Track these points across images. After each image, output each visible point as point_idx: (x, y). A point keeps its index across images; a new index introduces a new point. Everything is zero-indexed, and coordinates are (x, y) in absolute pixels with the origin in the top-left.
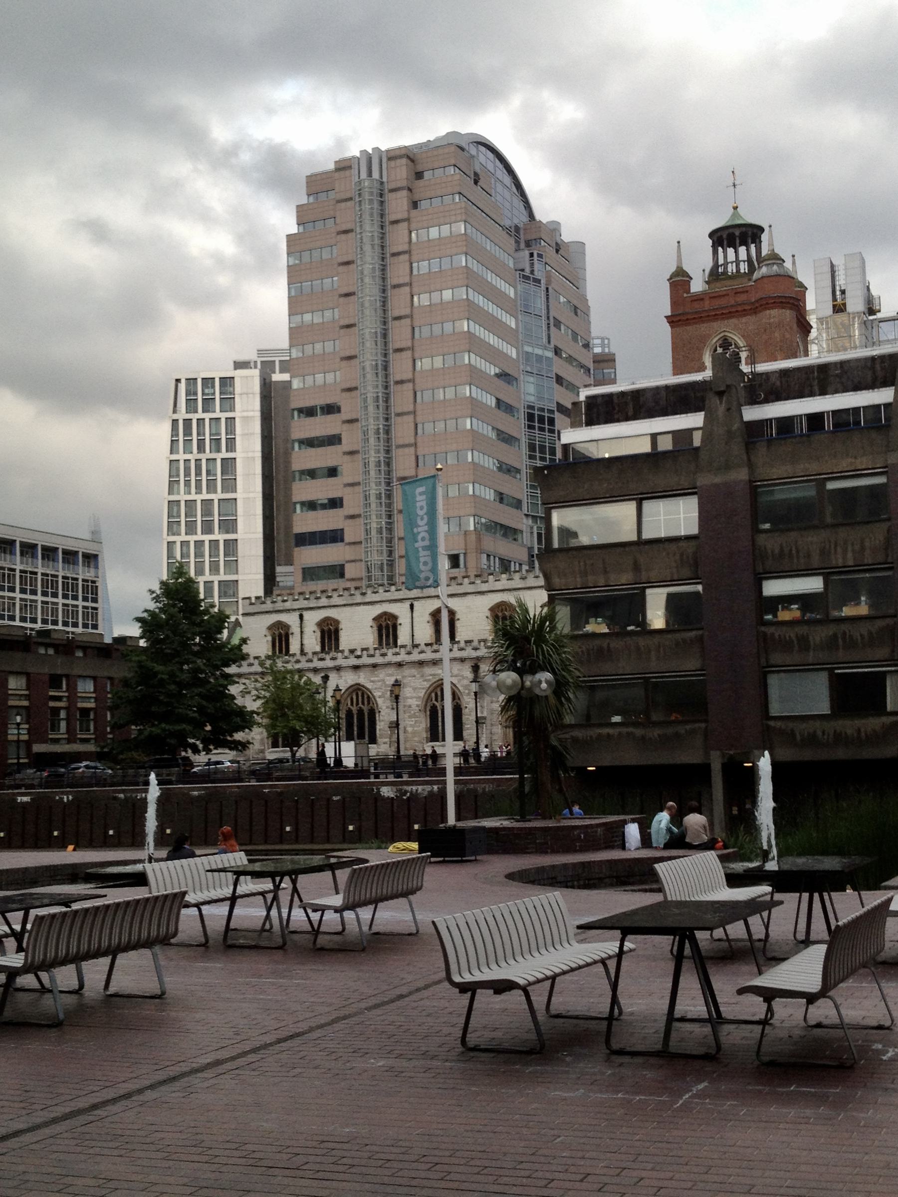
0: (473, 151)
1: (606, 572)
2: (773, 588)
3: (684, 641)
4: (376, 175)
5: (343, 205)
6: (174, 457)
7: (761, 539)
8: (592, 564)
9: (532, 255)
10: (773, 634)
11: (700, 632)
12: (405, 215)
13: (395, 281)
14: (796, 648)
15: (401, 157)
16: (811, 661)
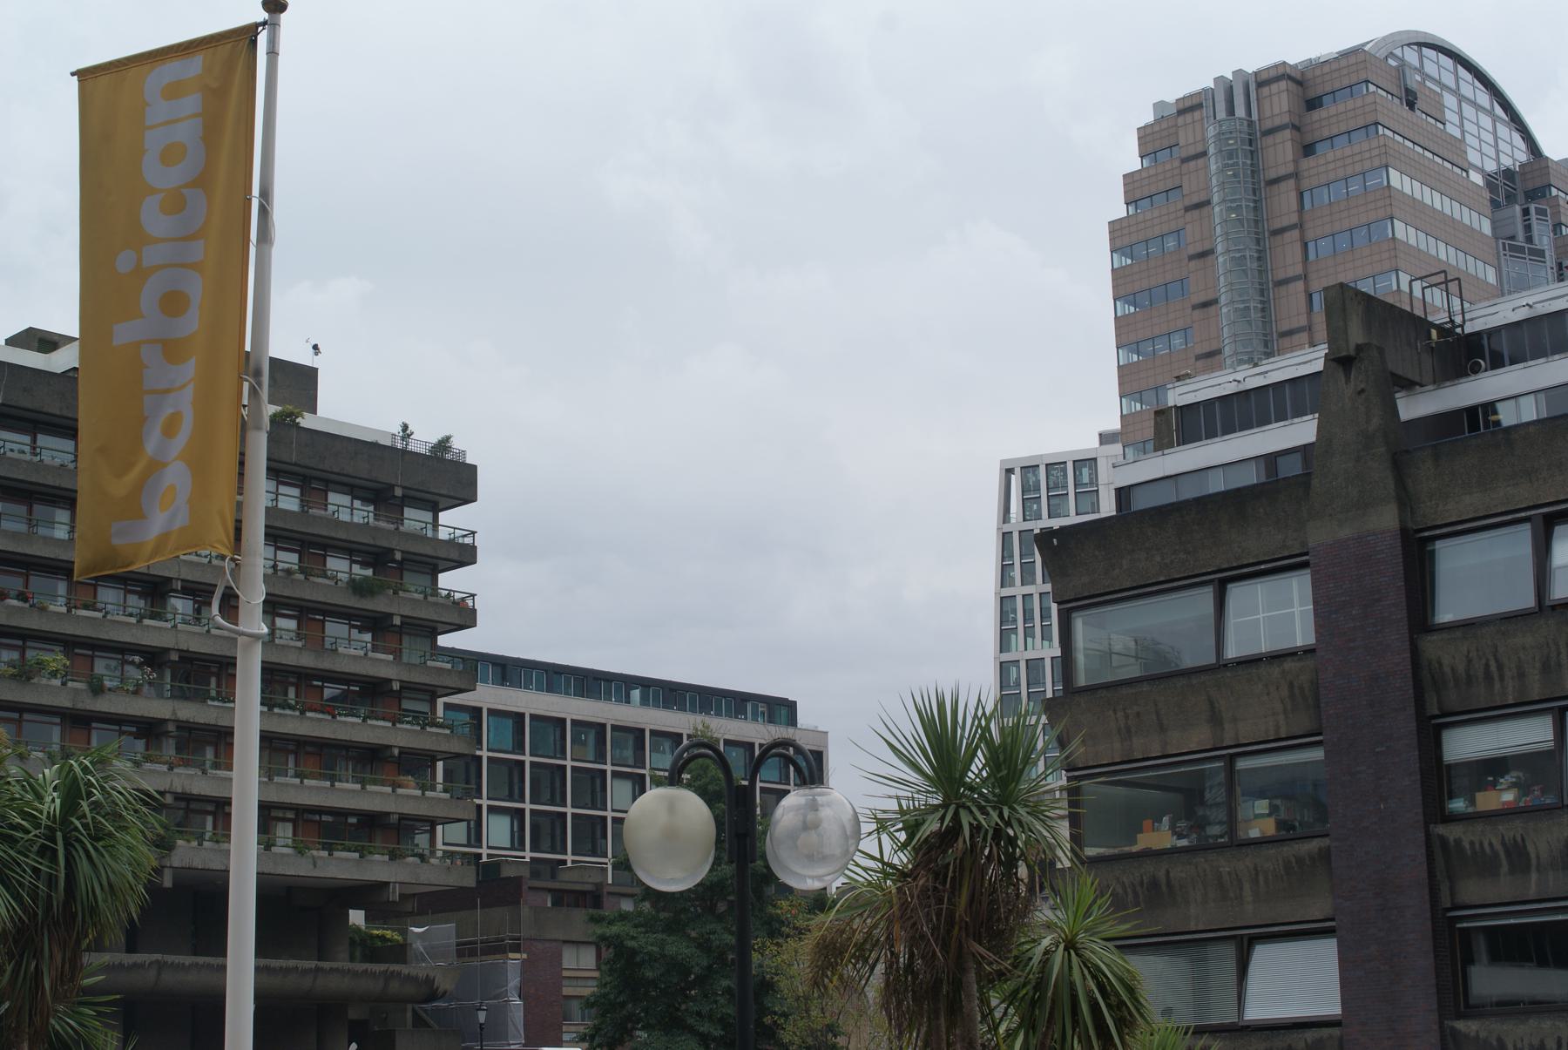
0: (1411, 56)
1: (1162, 729)
2: (1466, 744)
3: (1300, 860)
4: (1240, 111)
5: (1192, 164)
6: (1007, 592)
7: (1432, 646)
8: (1138, 714)
9: (1526, 212)
10: (1458, 842)
11: (1325, 842)
12: (1290, 169)
13: (1281, 275)
14: (1505, 868)
15: (1277, 79)
16: (1532, 893)
